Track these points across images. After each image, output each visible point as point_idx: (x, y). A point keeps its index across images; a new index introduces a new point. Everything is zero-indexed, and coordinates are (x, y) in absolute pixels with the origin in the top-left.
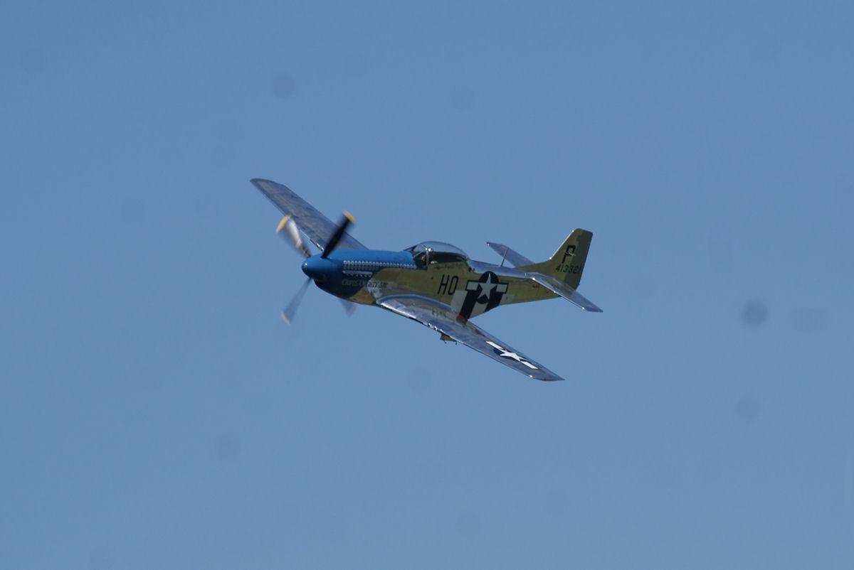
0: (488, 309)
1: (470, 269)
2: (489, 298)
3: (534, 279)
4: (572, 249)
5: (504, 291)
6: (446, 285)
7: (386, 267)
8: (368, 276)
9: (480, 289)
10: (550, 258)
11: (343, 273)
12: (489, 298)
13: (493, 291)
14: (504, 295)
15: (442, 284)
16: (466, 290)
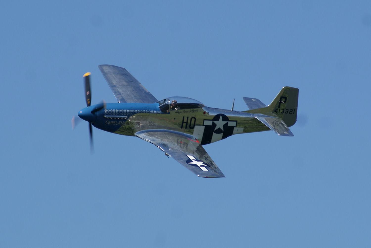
0: (224, 137)
1: (205, 113)
2: (223, 130)
3: (256, 117)
4: (284, 99)
5: (235, 125)
6: (187, 123)
7: (137, 113)
8: (124, 118)
9: (214, 125)
10: (269, 106)
11: (105, 118)
12: (223, 130)
13: (225, 126)
14: (235, 128)
15: (183, 122)
16: (203, 125)
